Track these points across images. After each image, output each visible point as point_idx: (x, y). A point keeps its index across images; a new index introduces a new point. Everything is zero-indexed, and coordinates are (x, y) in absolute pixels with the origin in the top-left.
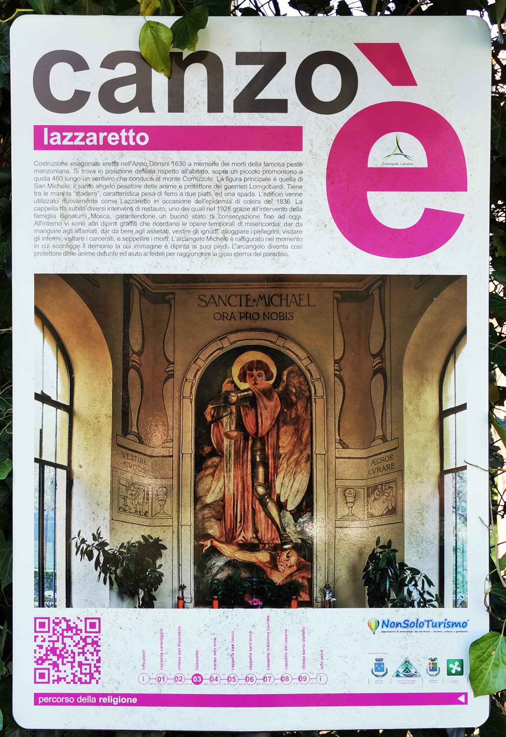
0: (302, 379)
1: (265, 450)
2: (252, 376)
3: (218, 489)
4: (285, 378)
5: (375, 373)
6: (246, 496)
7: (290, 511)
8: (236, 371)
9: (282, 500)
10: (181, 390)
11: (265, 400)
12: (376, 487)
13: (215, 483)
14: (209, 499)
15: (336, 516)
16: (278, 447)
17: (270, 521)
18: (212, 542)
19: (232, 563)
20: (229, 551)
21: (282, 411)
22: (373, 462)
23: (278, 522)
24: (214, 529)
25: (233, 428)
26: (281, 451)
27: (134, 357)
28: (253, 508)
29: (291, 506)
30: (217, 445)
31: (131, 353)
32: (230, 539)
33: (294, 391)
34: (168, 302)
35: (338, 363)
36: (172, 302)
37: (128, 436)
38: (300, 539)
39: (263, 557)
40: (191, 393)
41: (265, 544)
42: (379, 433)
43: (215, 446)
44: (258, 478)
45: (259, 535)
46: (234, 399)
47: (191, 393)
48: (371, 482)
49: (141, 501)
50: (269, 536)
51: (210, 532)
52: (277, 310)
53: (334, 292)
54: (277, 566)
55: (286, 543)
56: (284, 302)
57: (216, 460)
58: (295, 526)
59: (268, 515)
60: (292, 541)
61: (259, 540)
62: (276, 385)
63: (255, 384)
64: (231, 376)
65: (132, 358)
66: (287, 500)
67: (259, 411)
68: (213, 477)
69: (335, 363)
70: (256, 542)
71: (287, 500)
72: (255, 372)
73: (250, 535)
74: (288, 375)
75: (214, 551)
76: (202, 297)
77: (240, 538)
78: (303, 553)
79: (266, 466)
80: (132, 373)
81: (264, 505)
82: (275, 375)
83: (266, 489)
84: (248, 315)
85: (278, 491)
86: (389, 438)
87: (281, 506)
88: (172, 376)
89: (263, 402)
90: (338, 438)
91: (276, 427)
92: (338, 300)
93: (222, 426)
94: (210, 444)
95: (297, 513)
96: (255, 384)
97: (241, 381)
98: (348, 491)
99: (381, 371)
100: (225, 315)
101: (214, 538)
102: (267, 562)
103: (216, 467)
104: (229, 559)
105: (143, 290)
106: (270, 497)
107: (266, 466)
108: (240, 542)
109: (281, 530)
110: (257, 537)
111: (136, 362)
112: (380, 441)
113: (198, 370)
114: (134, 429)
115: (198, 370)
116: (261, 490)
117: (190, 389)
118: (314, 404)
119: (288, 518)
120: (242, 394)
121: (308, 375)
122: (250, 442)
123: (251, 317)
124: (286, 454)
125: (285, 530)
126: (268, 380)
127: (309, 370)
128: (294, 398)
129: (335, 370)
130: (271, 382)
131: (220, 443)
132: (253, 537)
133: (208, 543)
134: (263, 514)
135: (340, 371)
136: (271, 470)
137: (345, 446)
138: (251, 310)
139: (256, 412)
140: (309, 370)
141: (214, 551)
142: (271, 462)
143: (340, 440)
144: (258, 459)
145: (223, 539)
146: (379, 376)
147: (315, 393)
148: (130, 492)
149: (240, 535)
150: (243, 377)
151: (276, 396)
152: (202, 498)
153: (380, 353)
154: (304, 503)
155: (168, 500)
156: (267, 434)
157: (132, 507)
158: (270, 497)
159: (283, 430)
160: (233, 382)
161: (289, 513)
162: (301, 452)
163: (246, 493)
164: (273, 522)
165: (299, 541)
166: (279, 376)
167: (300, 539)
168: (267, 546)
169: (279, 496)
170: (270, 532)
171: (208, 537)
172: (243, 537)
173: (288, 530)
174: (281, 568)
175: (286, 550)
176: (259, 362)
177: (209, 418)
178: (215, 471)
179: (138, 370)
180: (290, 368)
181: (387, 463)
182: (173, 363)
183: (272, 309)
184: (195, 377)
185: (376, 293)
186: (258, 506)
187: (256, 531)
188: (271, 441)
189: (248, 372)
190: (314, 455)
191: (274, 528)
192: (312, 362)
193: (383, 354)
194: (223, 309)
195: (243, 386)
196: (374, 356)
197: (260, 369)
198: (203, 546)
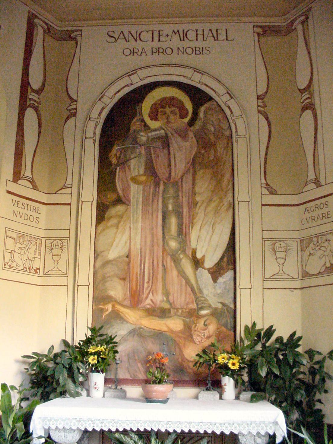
0: (221, 116)
1: (178, 196)
2: (165, 114)
3: (123, 242)
4: (201, 115)
5: (304, 109)
6: (155, 251)
7: (209, 270)
8: (146, 106)
9: (199, 256)
10: (84, 131)
11: (179, 139)
12: (311, 239)
13: (119, 235)
14: (112, 255)
15: (264, 274)
16: (194, 193)
17: (184, 281)
18: (113, 306)
19: (137, 333)
20: (133, 317)
21: (198, 152)
22: (306, 210)
23: (193, 281)
24: (117, 290)
25: (142, 172)
26: (198, 198)
27: (32, 96)
28: (163, 265)
29: (210, 263)
30: (123, 191)
31: (29, 90)
32: (135, 300)
33: (212, 129)
34: (74, 39)
35: (262, 99)
36: (79, 38)
37: (20, 182)
38: (221, 303)
39: (175, 324)
40: (95, 133)
41: (177, 309)
42: (312, 176)
43: (121, 193)
44: (170, 230)
45: (171, 298)
46: (144, 139)
47: (95, 133)
48: (305, 234)
49: (31, 256)
50: (183, 299)
51: (112, 293)
52: (193, 44)
53: (254, 26)
54: (191, 336)
55: (202, 308)
56: (200, 37)
57: (120, 208)
58: (214, 288)
59: (182, 273)
60: (210, 306)
61: (171, 304)
62: (191, 123)
63: (168, 122)
64: (141, 114)
65: (30, 97)
66: (204, 256)
67: (172, 152)
68: (117, 228)
69: (258, 99)
70: (167, 306)
71: (204, 256)
72: (167, 110)
73: (159, 298)
74: (205, 113)
75: (116, 316)
76: (110, 34)
77: (148, 301)
78: (224, 320)
79: (179, 215)
80: (30, 113)
81: (176, 261)
82: (190, 115)
83: (180, 243)
84: (161, 50)
85: (193, 245)
86: (323, 183)
87: (197, 263)
88: (75, 115)
89: (175, 142)
90: (263, 181)
91: (191, 171)
92: (259, 35)
93: (129, 169)
94: (115, 190)
95: (216, 273)
96: (168, 122)
97: (151, 119)
98: (277, 245)
99: (310, 107)
100: (136, 50)
101: (116, 301)
102: (181, 331)
103: (121, 217)
104: (134, 327)
105: (48, 29)
106: (184, 252)
107: (179, 215)
108: (148, 306)
109: (195, 292)
110: (168, 300)
111: (35, 101)
112: (314, 186)
113: (103, 108)
114: (28, 173)
115: (103, 108)
116: (173, 244)
117: (94, 129)
118: (235, 145)
119: (205, 277)
120: (153, 133)
121: (228, 113)
122: (162, 188)
123: (164, 52)
124: (203, 201)
125: (201, 292)
126: (182, 117)
127: (229, 107)
128: (212, 138)
129: (258, 106)
130: (187, 120)
131: (126, 189)
132: (163, 301)
133: (109, 307)
134: (175, 273)
135: (265, 106)
136: (185, 220)
137: (272, 192)
138: (164, 45)
139: (169, 152)
140: (229, 107)
141: (116, 316)
142: (185, 210)
143: (267, 184)
144: (170, 207)
145: (127, 303)
146: (308, 113)
147: (236, 131)
148: (18, 245)
149: (147, 298)
150: (154, 116)
151: (191, 135)
152: (103, 254)
153: (308, 88)
154: (225, 259)
155: (64, 255)
156: (182, 178)
157: (20, 263)
158: (184, 252)
159: (200, 174)
160: (143, 121)
161: (206, 271)
162: (221, 199)
163: (155, 248)
164: (188, 282)
165: (220, 306)
166: (195, 113)
167: (221, 303)
168: (180, 311)
169: (194, 252)
170: (184, 295)
171: (107, 299)
172: (152, 300)
173: (205, 292)
174: (197, 339)
175: (203, 316)
176: (173, 99)
177: (114, 161)
178: (119, 222)
179: (36, 109)
180: (207, 105)
181: (322, 211)
182: (76, 101)
183: (186, 44)
184: (99, 115)
185: (300, 27)
186: (169, 263)
187: (167, 294)
188: (187, 186)
189: (160, 110)
190: (236, 202)
191: (189, 289)
192: (232, 98)
193: (311, 89)
194: (132, 44)
195: (153, 124)
196: (302, 91)
197: (174, 106)
198: (102, 311)
